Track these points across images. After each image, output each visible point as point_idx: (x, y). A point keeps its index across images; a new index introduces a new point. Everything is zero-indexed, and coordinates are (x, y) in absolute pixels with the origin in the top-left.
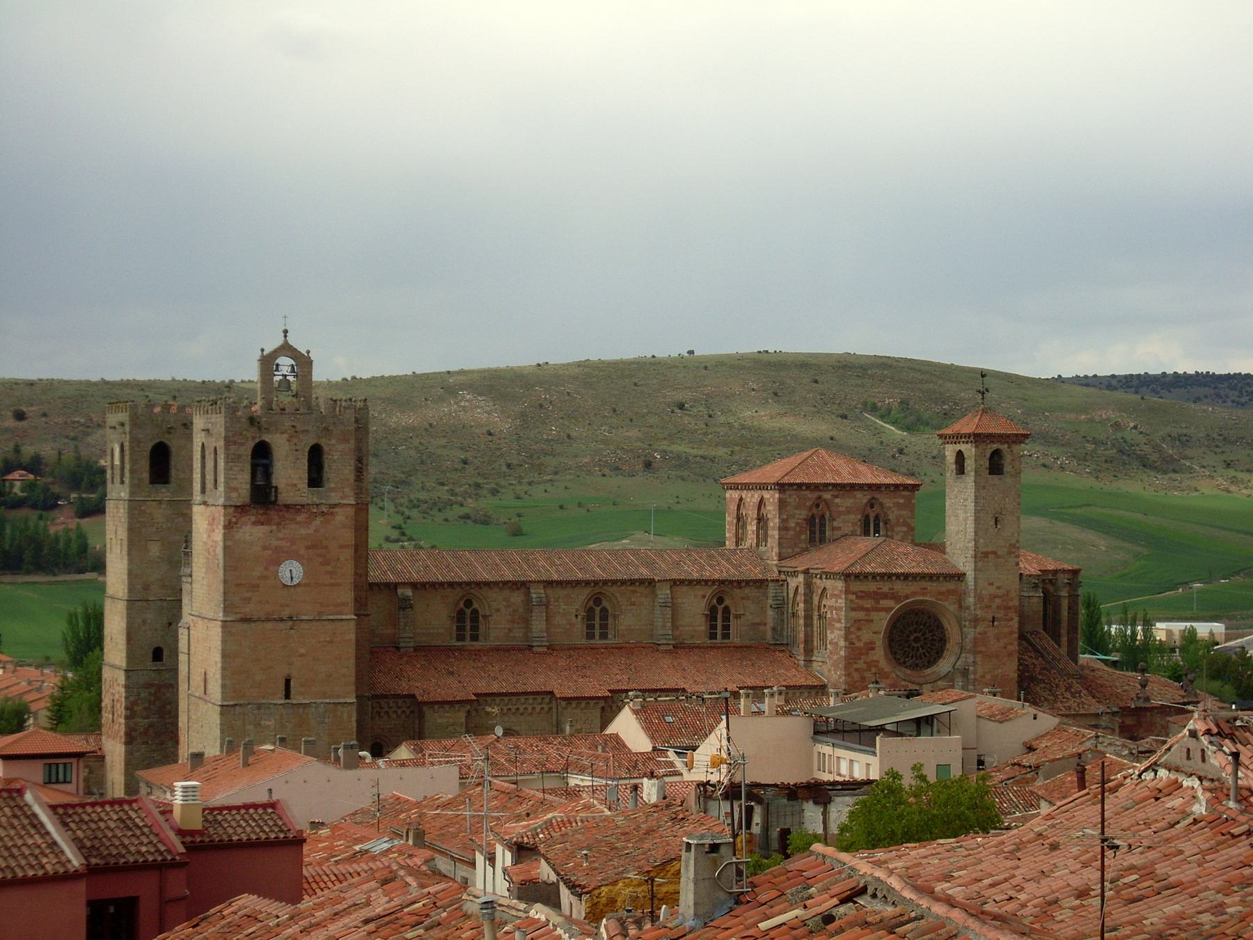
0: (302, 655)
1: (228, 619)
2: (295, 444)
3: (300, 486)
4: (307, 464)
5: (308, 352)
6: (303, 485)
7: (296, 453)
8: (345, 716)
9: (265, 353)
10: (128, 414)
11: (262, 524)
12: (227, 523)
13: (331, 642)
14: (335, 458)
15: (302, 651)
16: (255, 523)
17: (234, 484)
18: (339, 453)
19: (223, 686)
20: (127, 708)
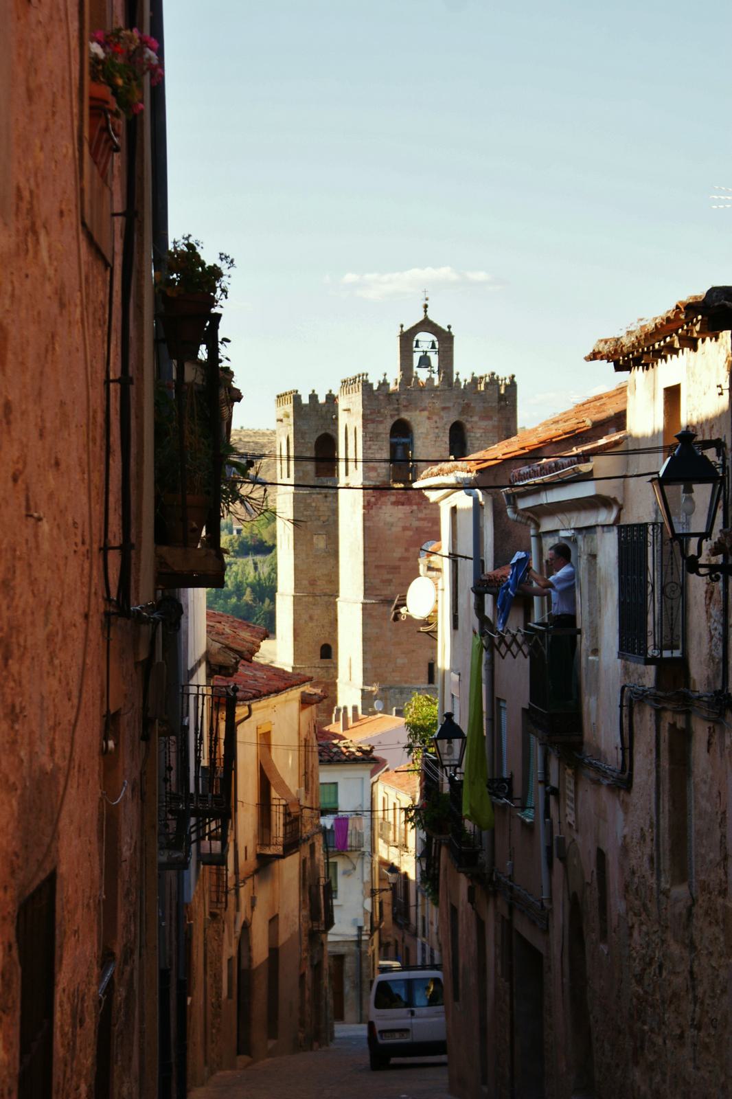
1: (368, 601)
2: (436, 422)
4: (448, 442)
5: (449, 327)
7: (437, 431)
9: (405, 329)
10: (292, 404)
11: (403, 504)
12: (366, 504)
14: (478, 435)
16: (396, 503)
18: (481, 431)
19: (365, 671)
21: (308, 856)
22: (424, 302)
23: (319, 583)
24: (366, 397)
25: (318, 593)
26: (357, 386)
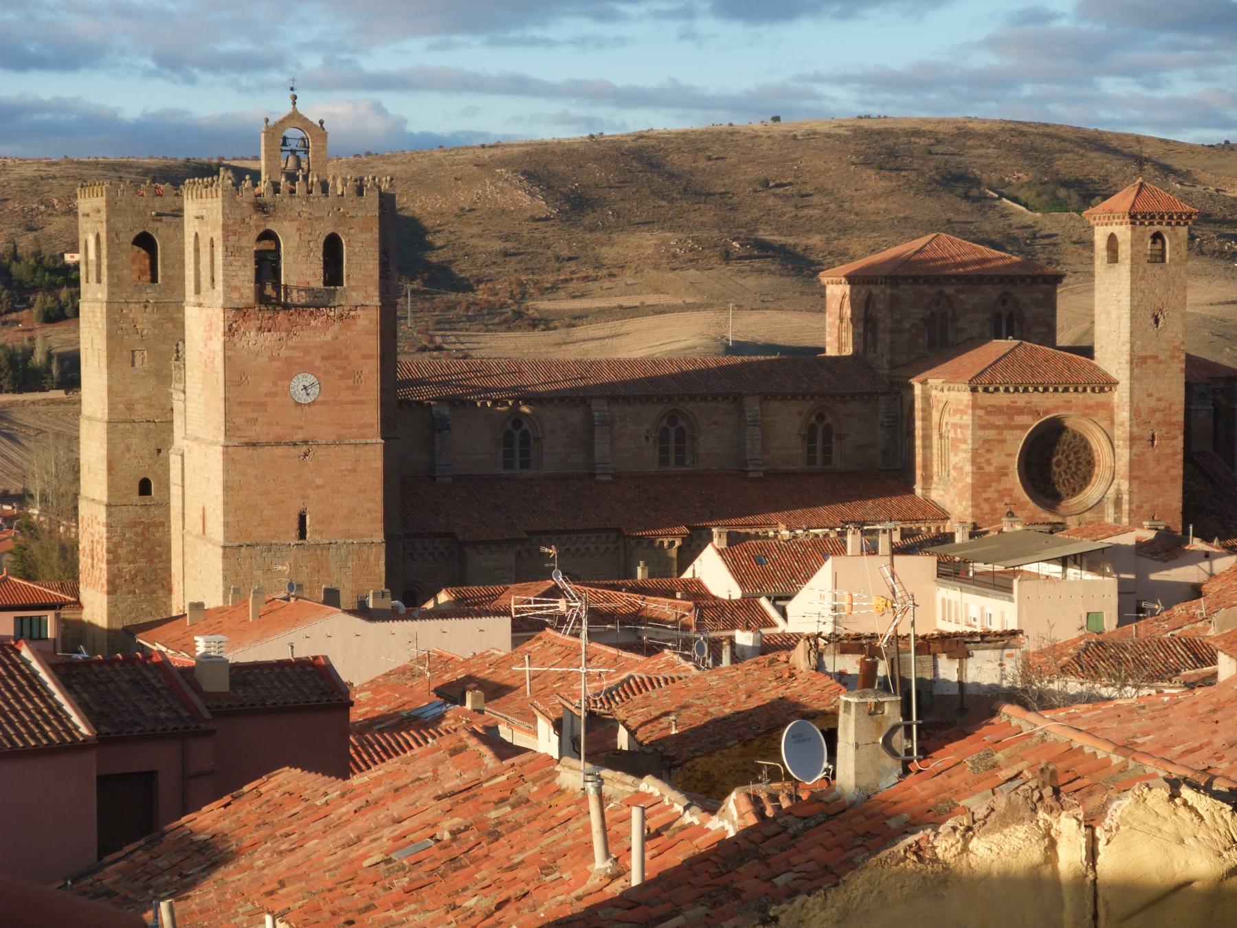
0: (318, 487)
1: (230, 444)
4: (322, 259)
5: (321, 122)
8: (372, 558)
9: (271, 123)
10: (104, 198)
12: (227, 329)
13: (354, 470)
15: (319, 481)
18: (360, 245)
20: (109, 551)
23: (137, 407)
24: (226, 205)
25: (137, 418)
26: (214, 191)
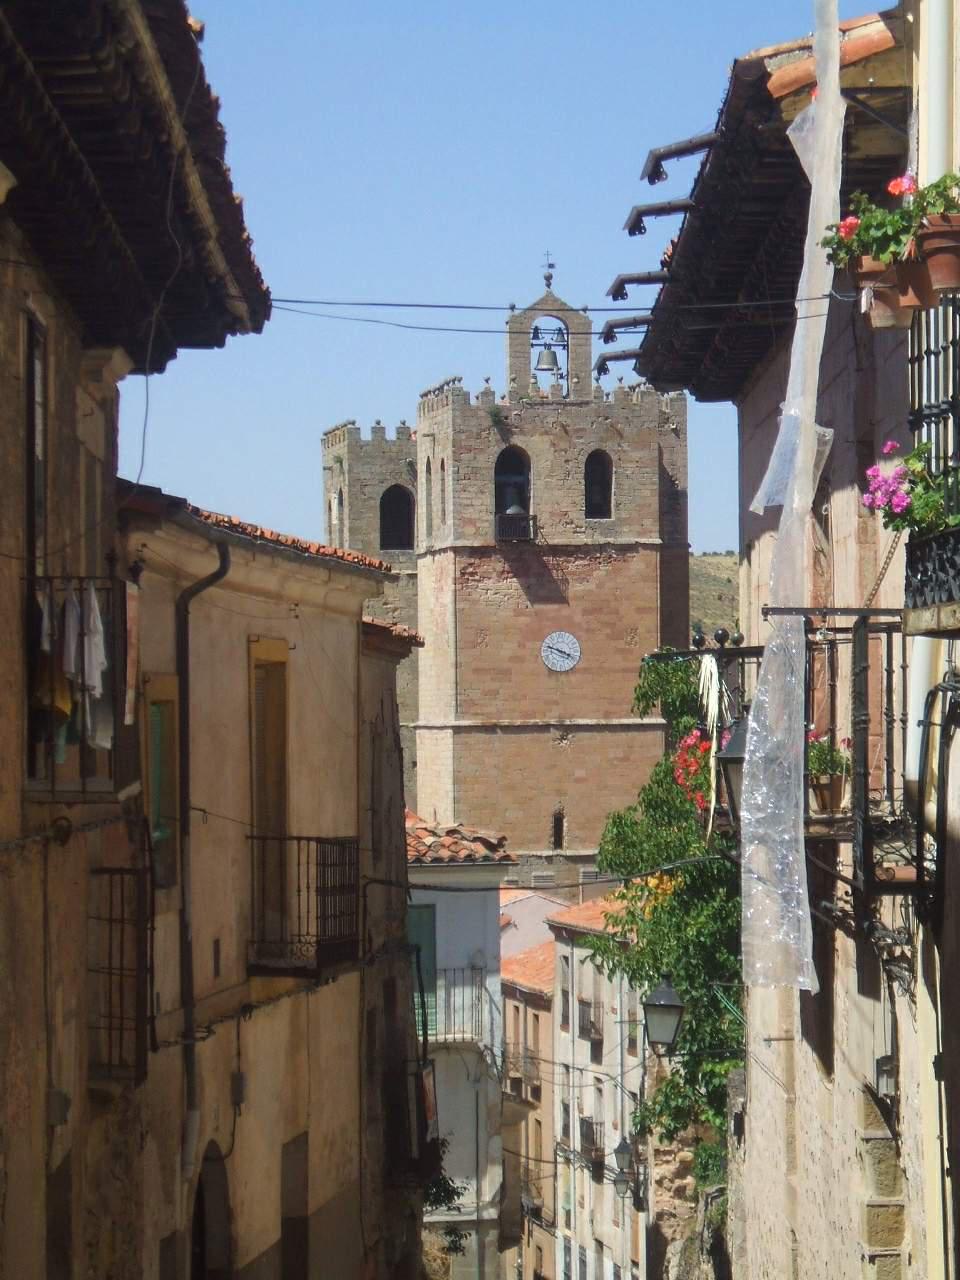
0: (578, 780)
3: (572, 515)
4: (583, 482)
6: (578, 514)
10: (346, 443)
13: (626, 759)
15: (580, 773)
17: (469, 513)
21: (381, 1003)
22: (546, 271)
